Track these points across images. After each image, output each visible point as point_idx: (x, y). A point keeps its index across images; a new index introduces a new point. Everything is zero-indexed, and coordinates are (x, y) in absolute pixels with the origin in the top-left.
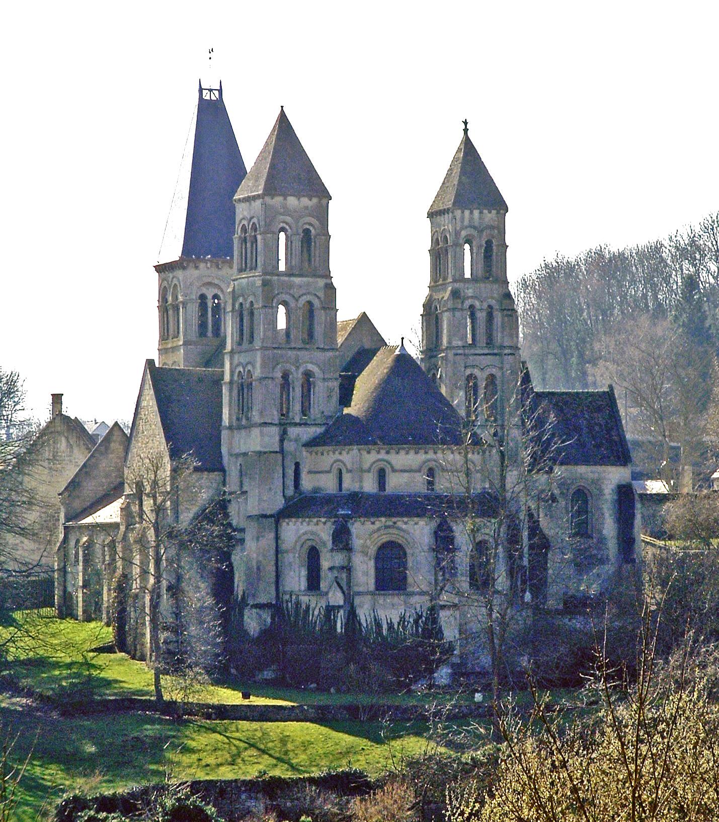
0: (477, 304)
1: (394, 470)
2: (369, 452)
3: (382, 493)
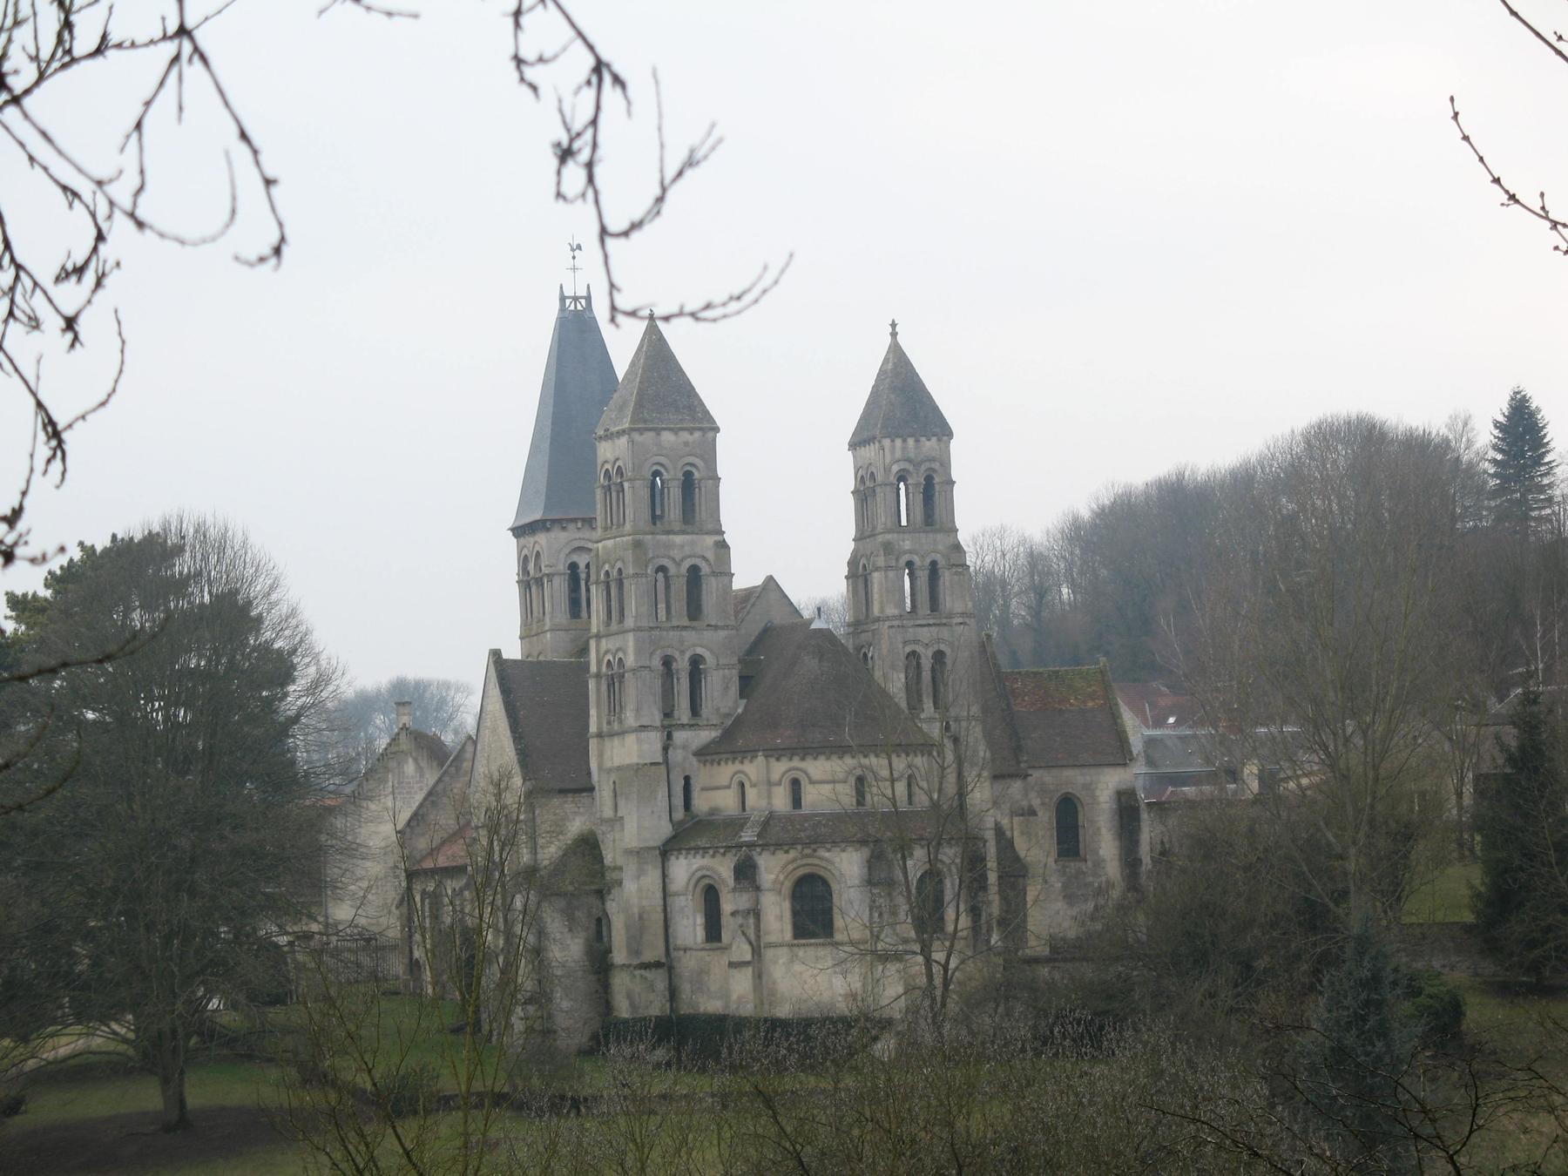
0: (916, 559)
2: (778, 759)
3: (798, 812)
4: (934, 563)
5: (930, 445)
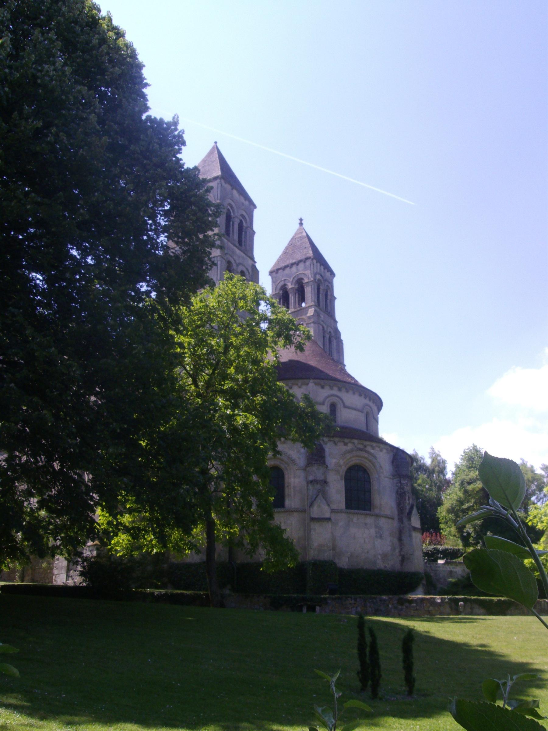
1: (345, 407)
2: (323, 387)
4: (330, 332)
5: (328, 274)
